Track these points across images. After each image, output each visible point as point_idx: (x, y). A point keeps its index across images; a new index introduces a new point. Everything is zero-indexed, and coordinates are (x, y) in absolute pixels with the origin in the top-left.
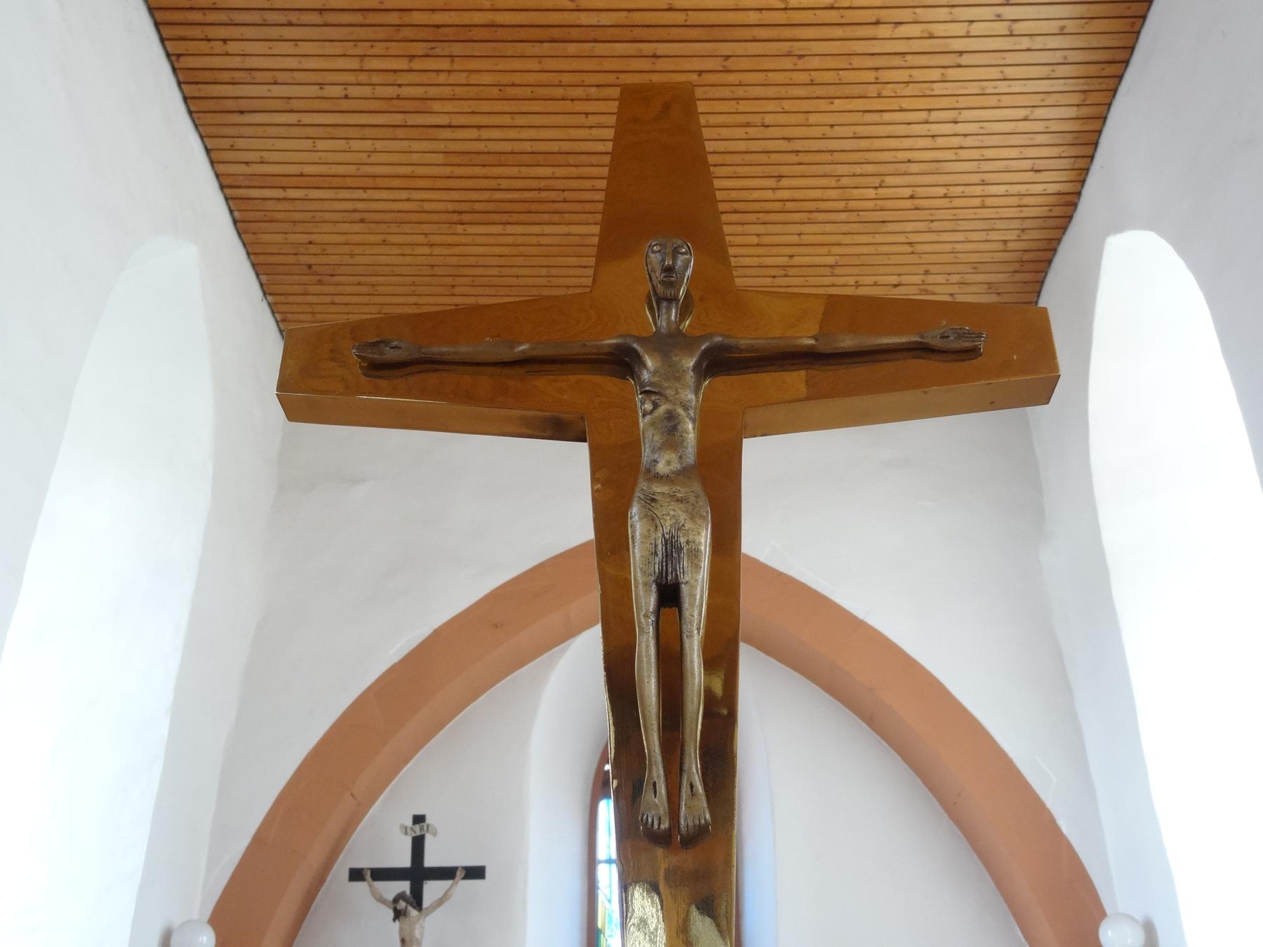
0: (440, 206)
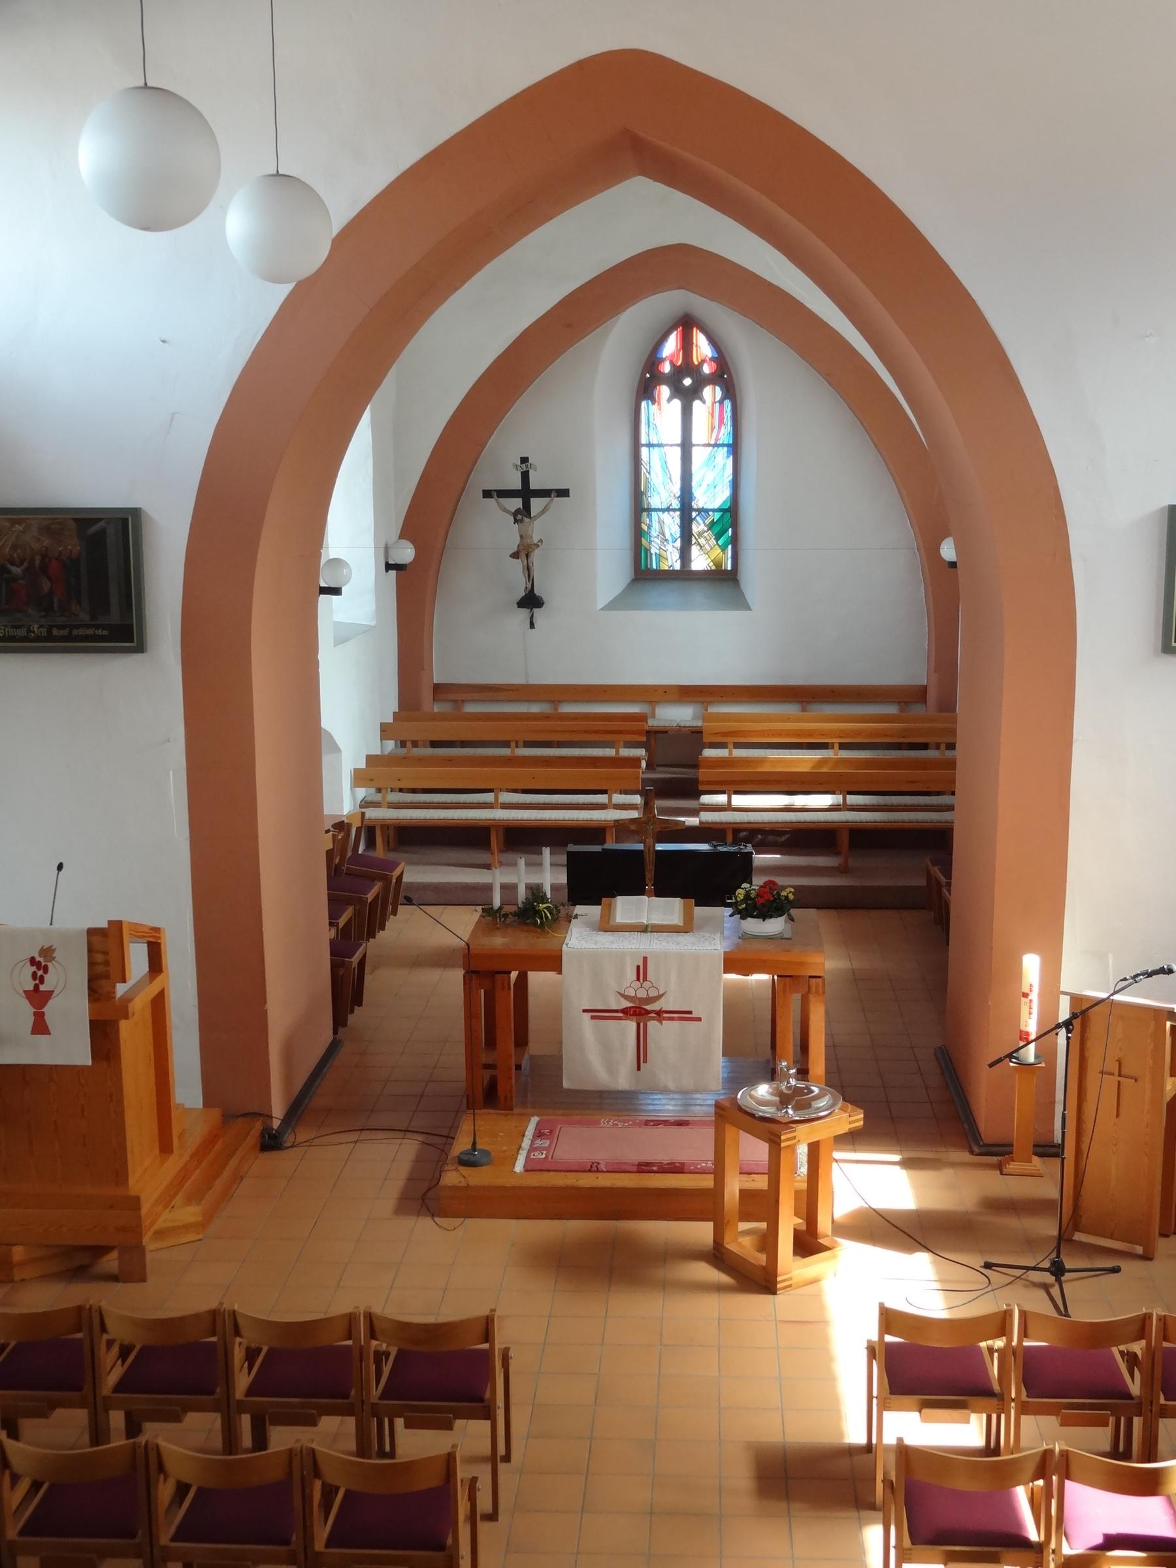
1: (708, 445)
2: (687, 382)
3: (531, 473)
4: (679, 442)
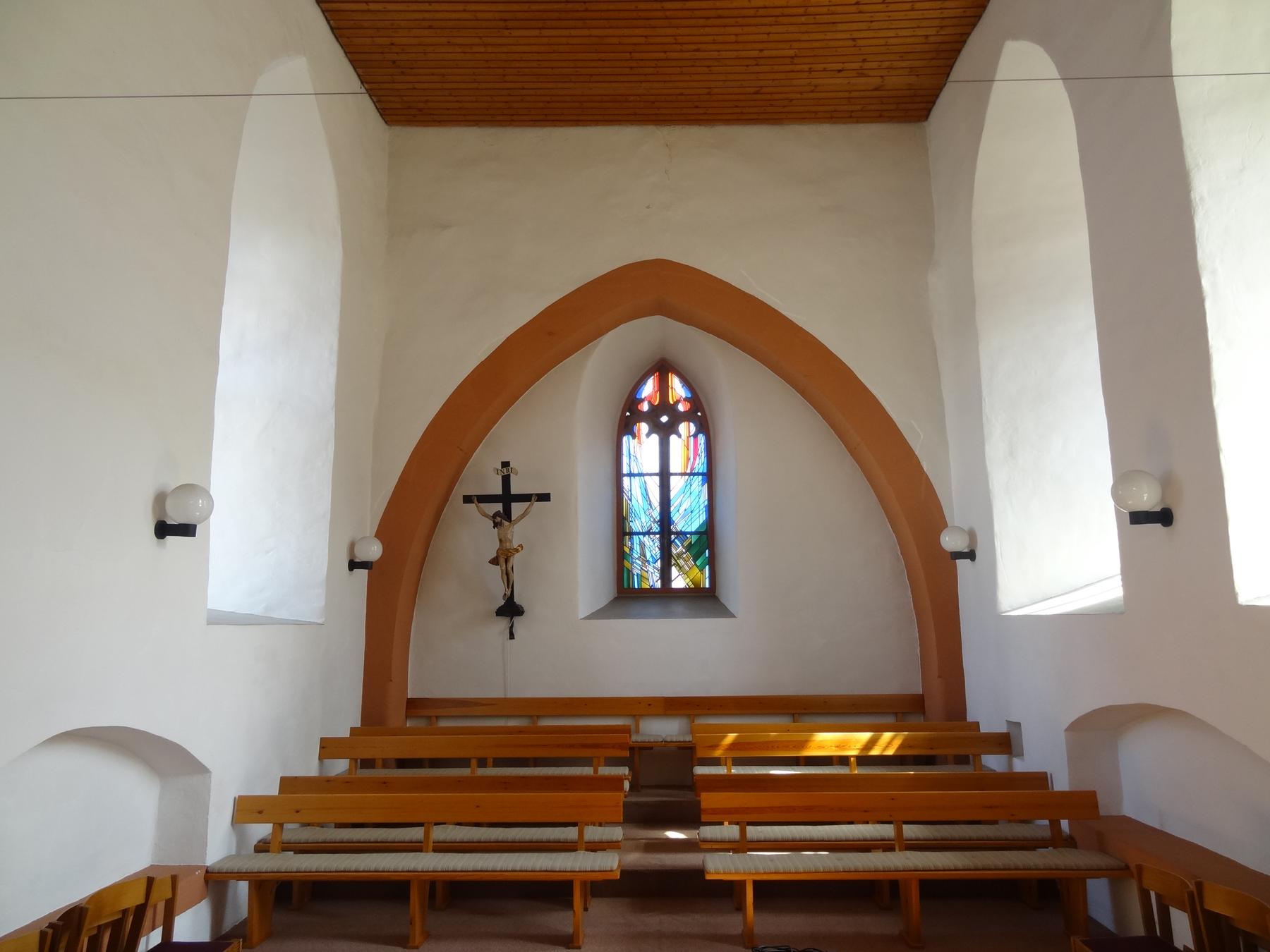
0: (490, 16)
1: (685, 474)
3: (513, 477)
4: (657, 471)
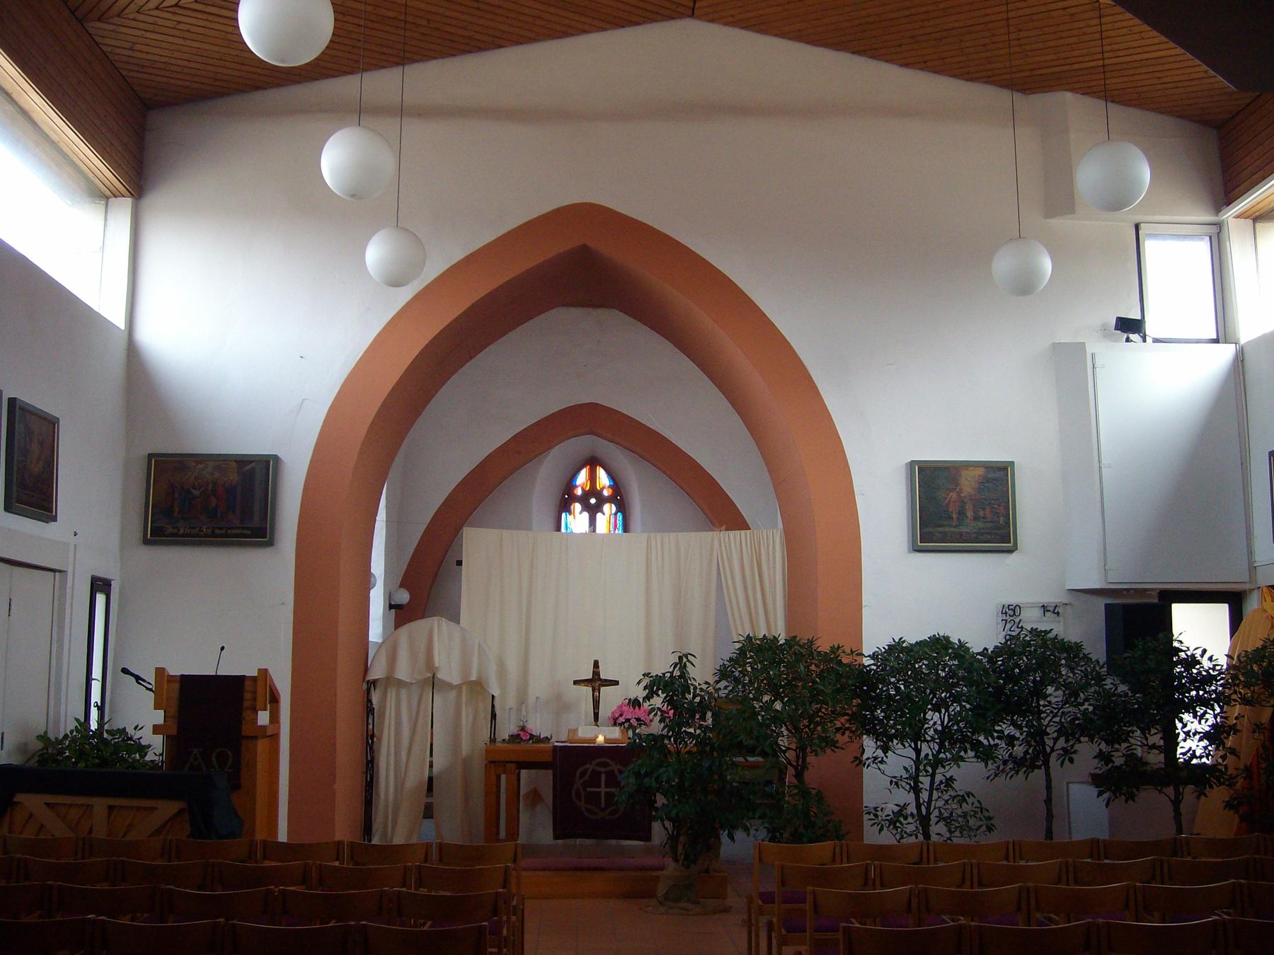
2: (593, 501)
